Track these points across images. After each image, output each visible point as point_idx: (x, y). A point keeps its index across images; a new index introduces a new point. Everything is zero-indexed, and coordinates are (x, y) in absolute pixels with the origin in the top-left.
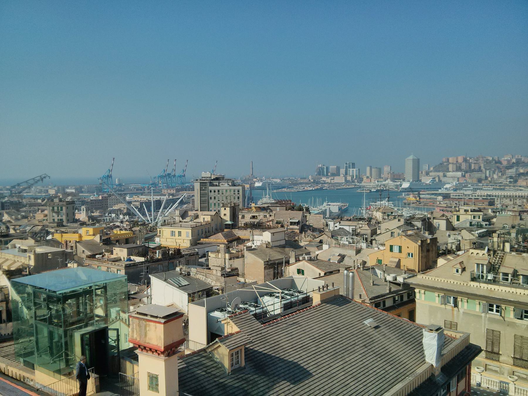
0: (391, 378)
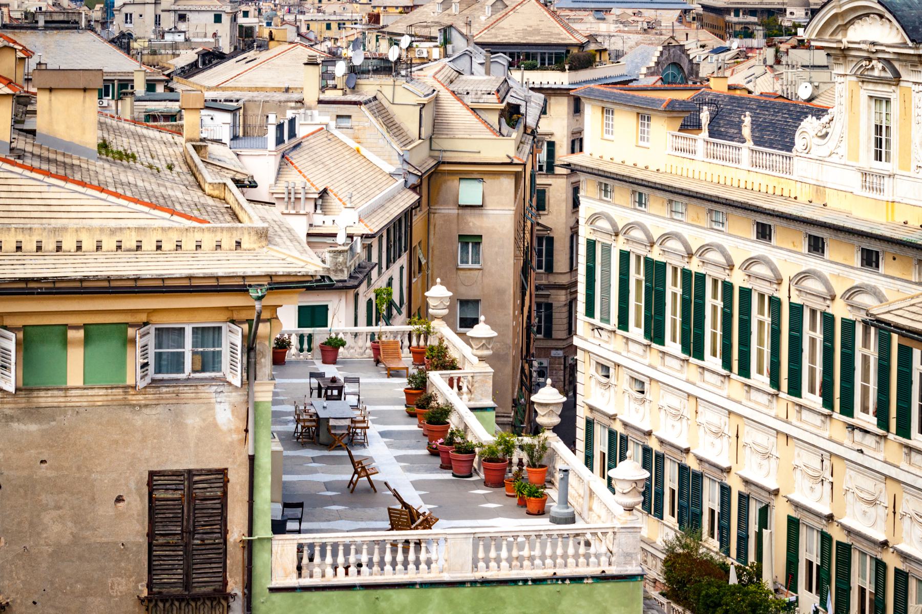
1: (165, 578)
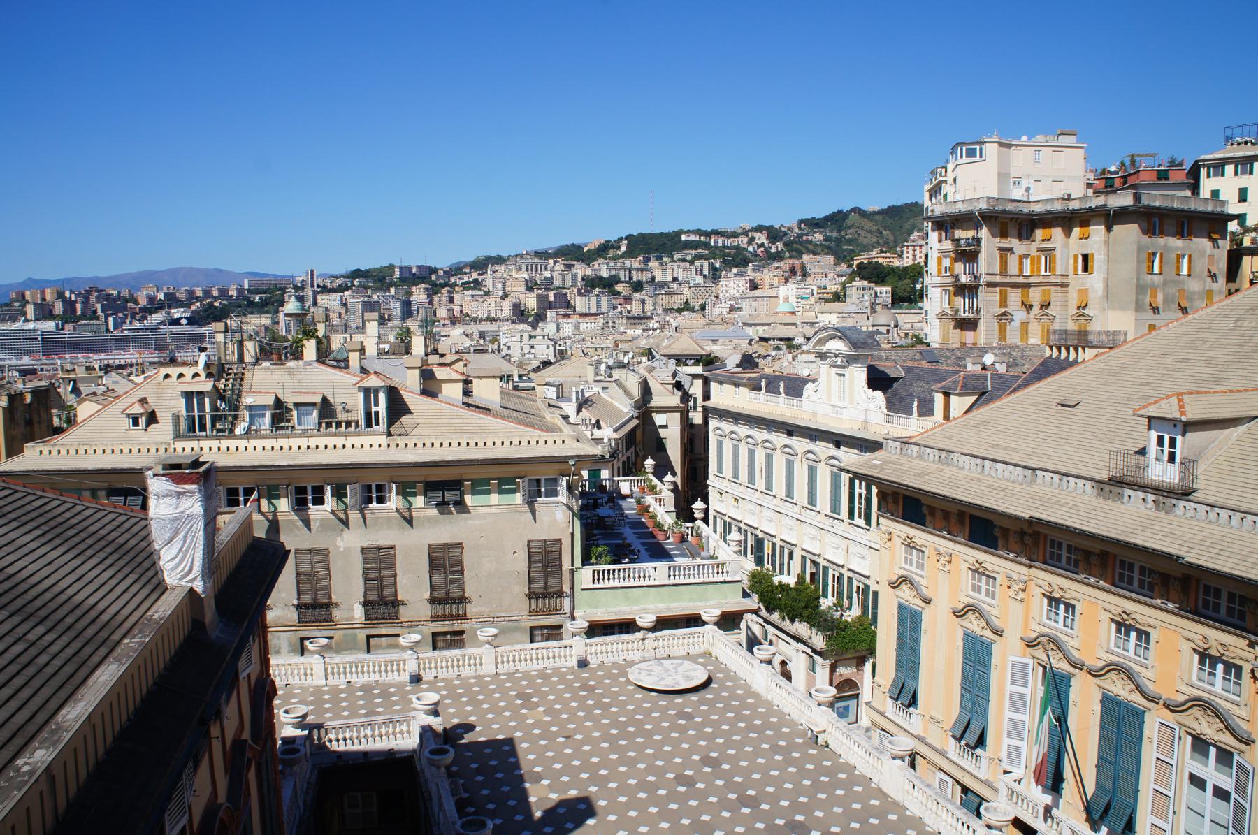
0: (57, 662)
1: (536, 585)
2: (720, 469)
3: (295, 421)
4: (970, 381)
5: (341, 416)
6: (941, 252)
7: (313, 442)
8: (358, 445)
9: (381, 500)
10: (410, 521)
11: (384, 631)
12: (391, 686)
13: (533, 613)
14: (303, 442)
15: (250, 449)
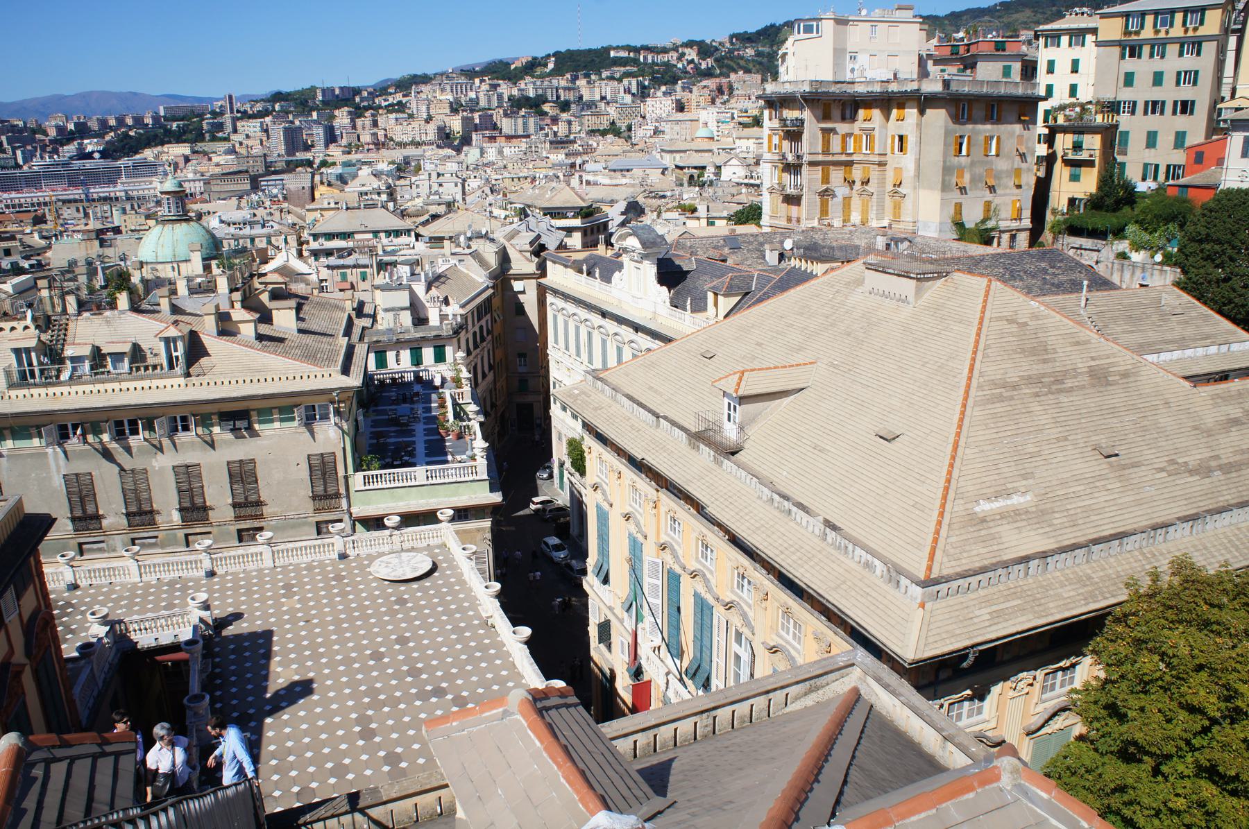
2: (556, 342)
3: (110, 367)
4: (736, 282)
5: (151, 360)
6: (772, 129)
7: (124, 385)
8: (161, 386)
9: (186, 428)
10: (212, 445)
11: (198, 530)
12: (191, 580)
13: (317, 511)
14: (116, 386)
15: (73, 393)
